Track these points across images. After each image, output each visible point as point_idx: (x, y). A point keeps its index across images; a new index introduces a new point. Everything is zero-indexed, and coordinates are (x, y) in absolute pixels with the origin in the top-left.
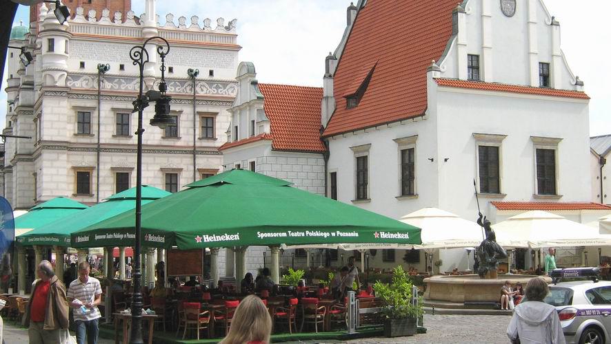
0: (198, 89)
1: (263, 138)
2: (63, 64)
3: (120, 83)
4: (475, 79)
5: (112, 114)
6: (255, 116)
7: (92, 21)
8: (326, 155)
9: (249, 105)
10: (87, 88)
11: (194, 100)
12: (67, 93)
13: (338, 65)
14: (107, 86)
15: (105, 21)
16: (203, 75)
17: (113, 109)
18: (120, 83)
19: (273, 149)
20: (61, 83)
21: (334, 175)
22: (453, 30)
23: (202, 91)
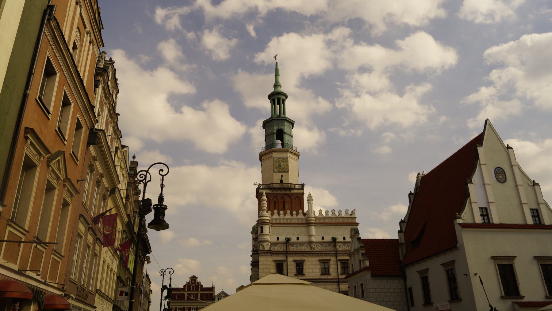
0: (338, 247)
1: (366, 269)
2: (268, 238)
3: (297, 247)
4: (487, 224)
5: (293, 263)
6: (361, 258)
7: (282, 216)
8: (404, 277)
9: (357, 251)
10: (281, 250)
11: (336, 253)
12: (270, 253)
13: (407, 225)
14: (291, 248)
15: (288, 216)
16: (340, 239)
17: (294, 261)
18: (297, 247)
19: (373, 276)
20: (267, 248)
21: (410, 289)
22: (466, 195)
23: (340, 248)
